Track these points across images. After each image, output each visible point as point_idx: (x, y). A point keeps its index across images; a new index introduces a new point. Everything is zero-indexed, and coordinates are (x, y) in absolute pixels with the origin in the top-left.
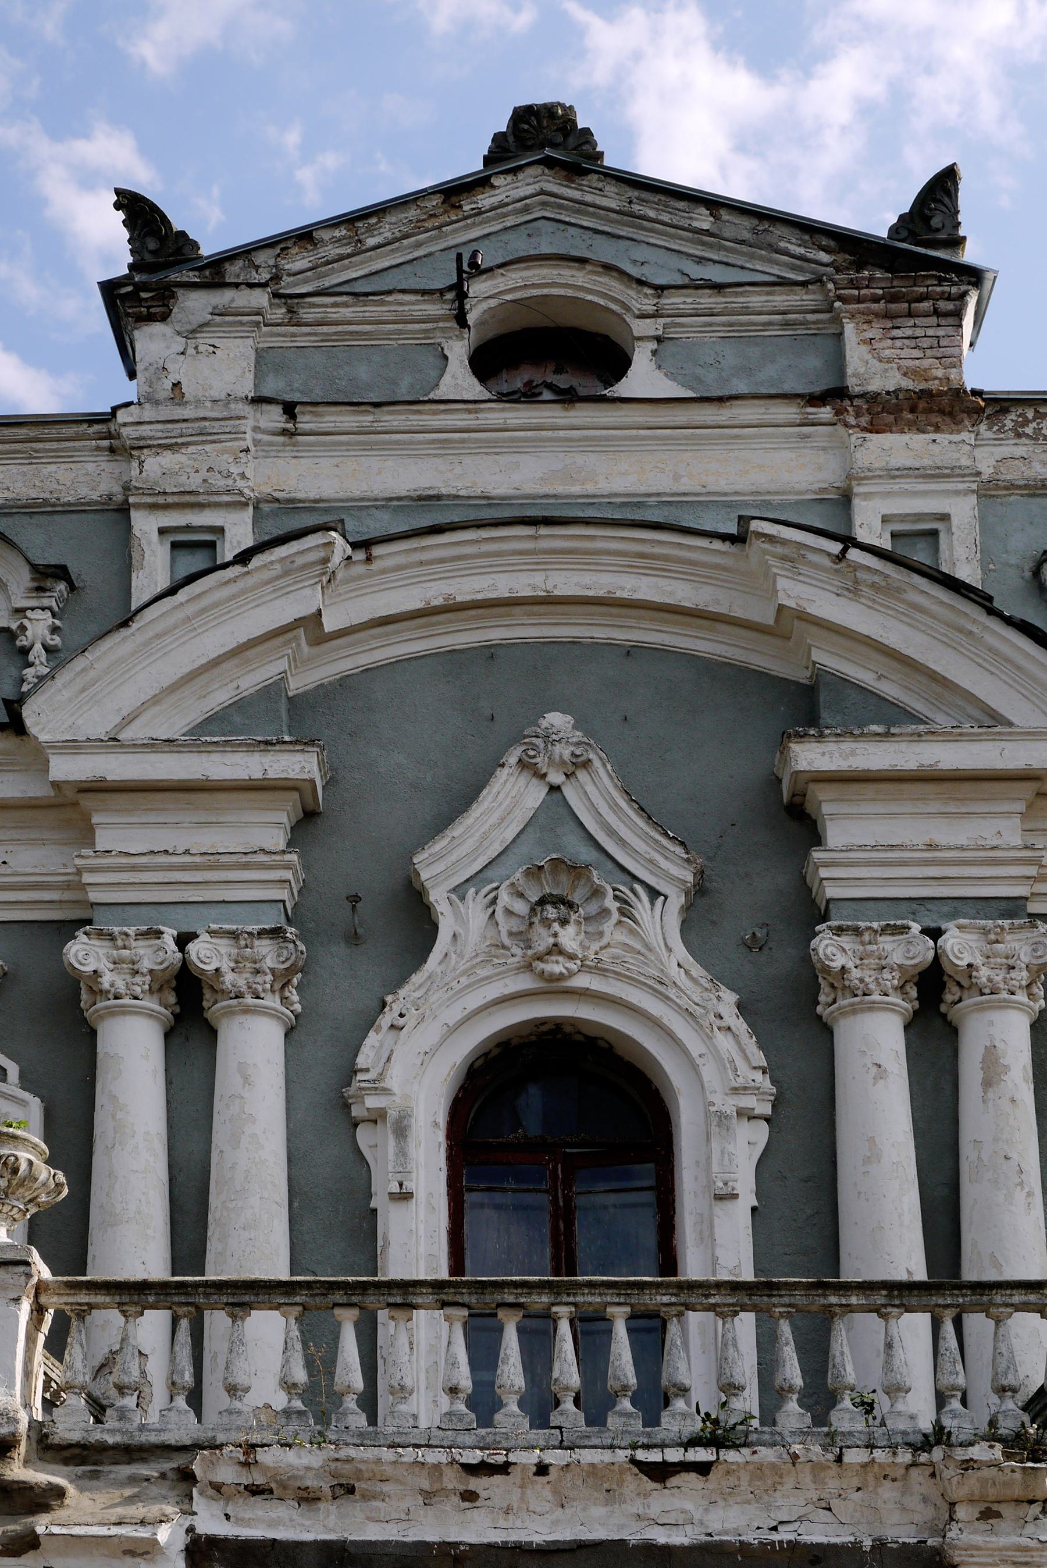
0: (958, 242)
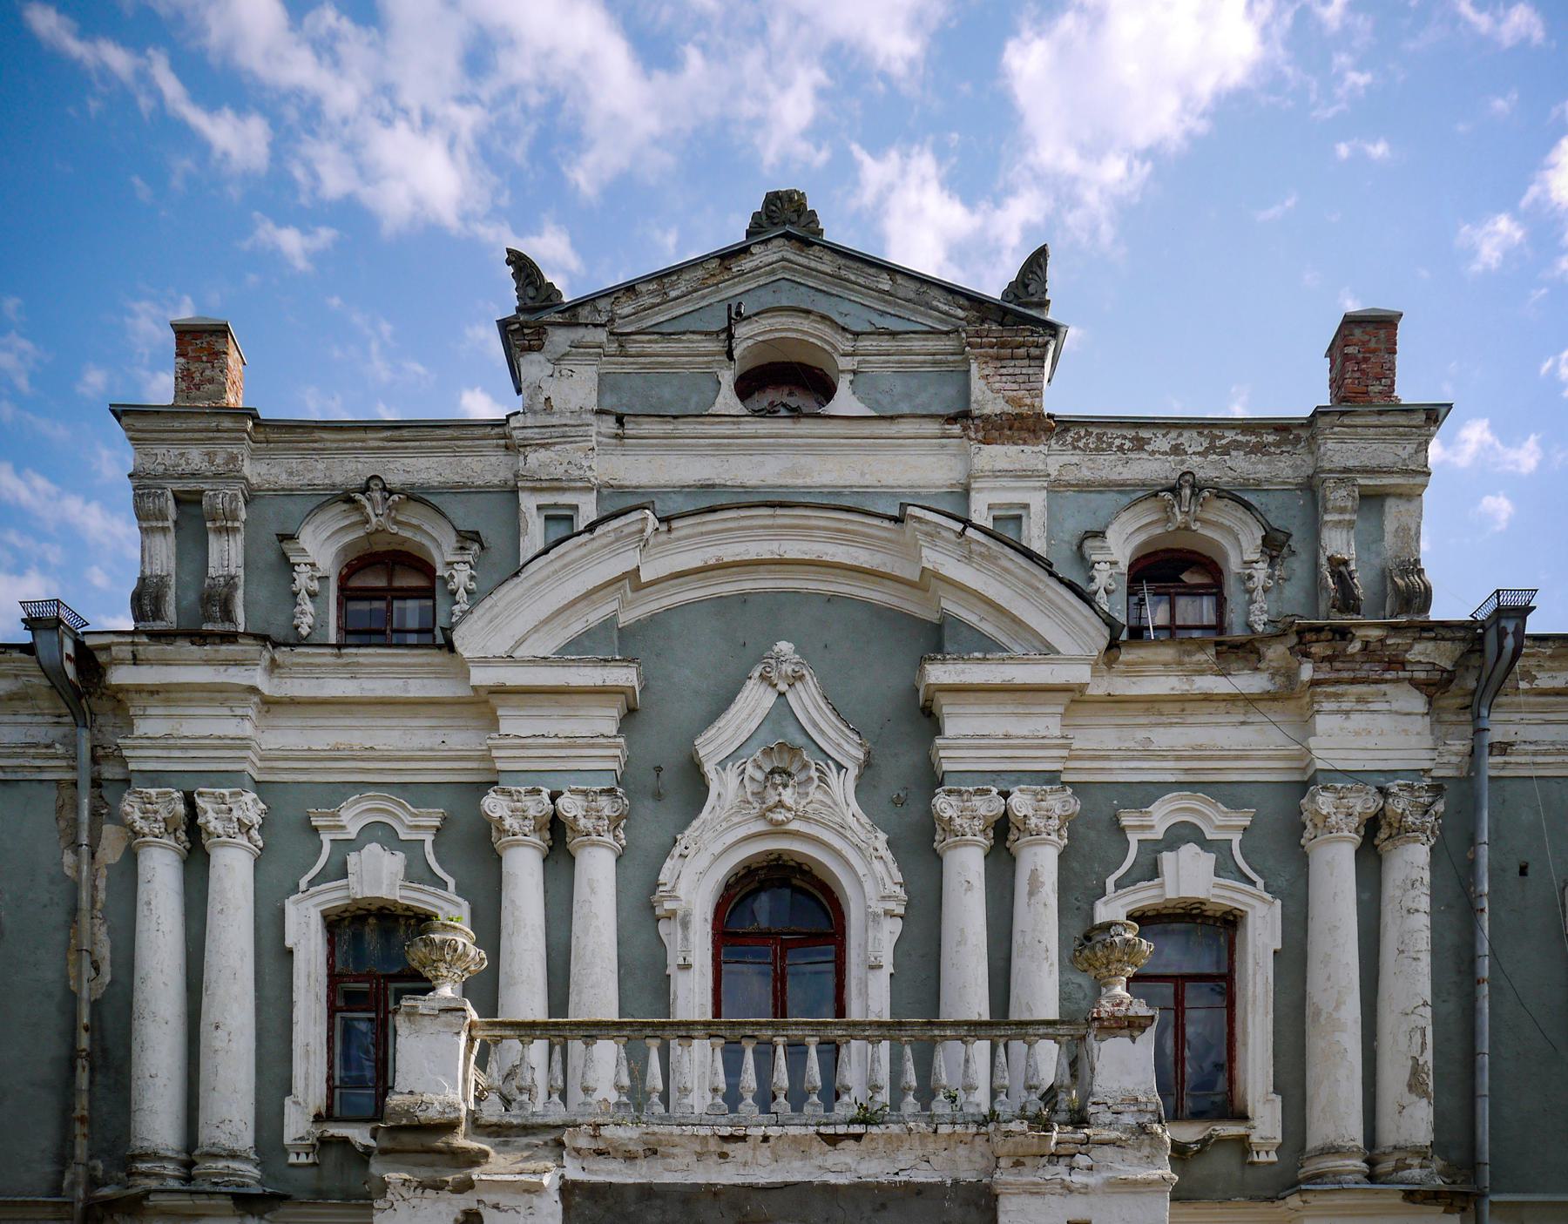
0: (1044, 304)
